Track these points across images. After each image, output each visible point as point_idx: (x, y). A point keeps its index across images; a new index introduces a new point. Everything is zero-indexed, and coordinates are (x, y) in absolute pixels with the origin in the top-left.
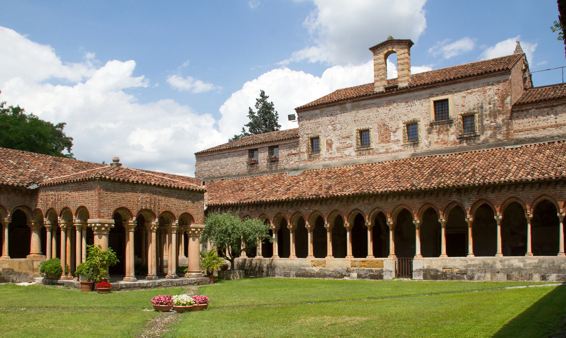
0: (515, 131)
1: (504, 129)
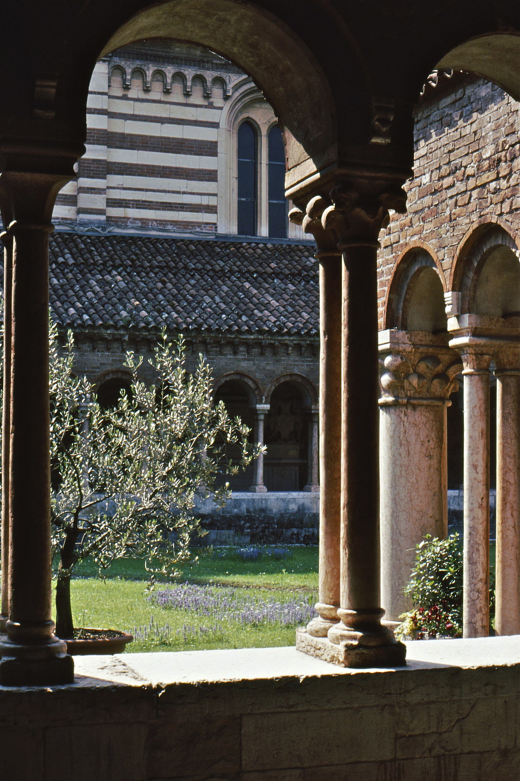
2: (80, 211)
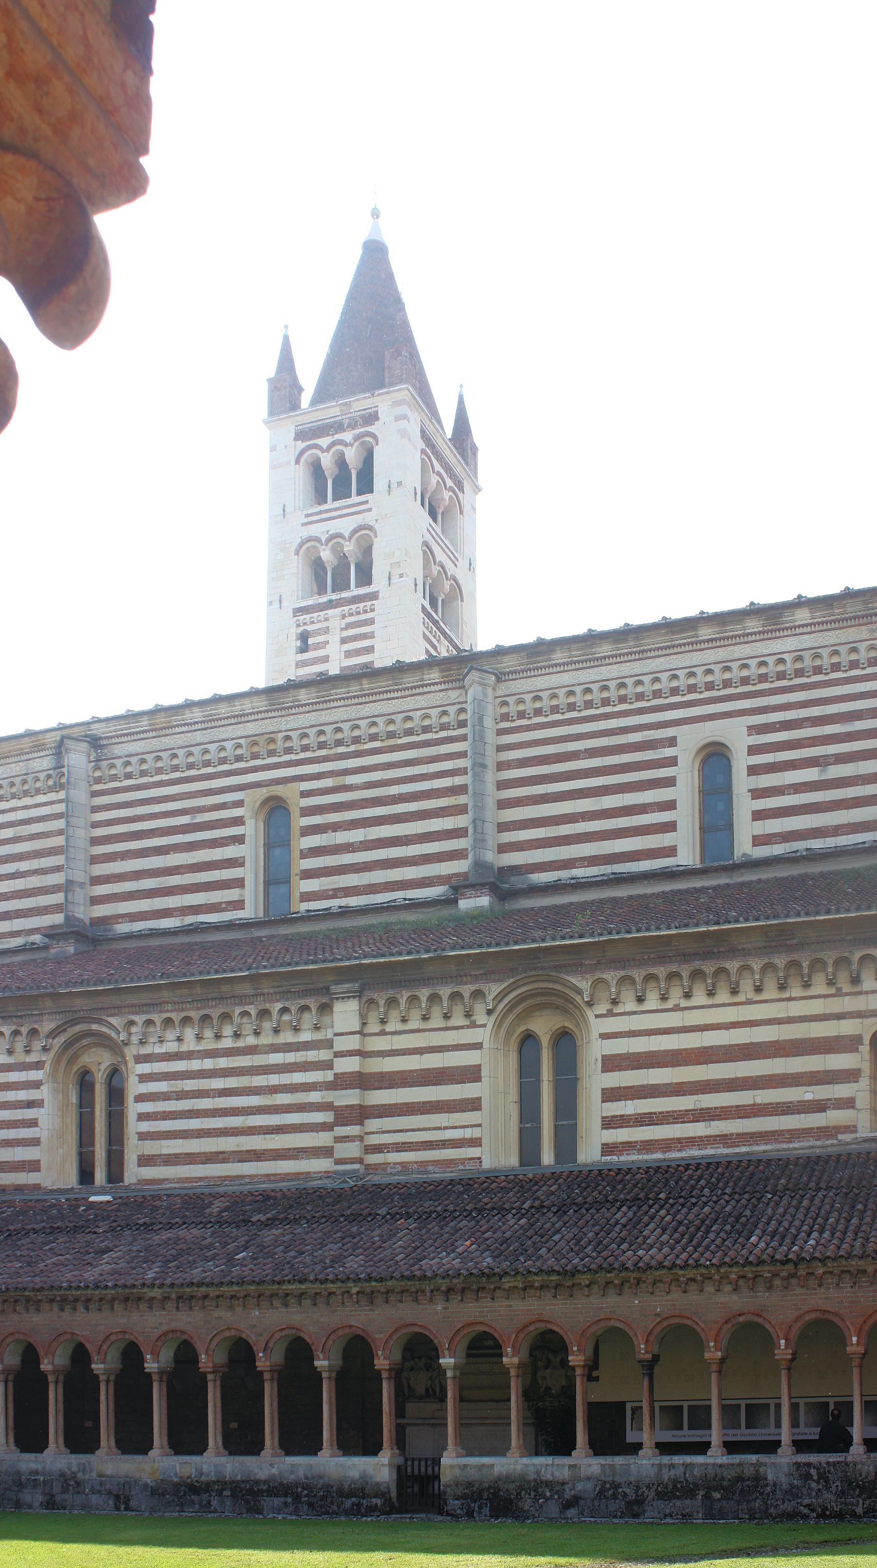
2: (338, 1162)
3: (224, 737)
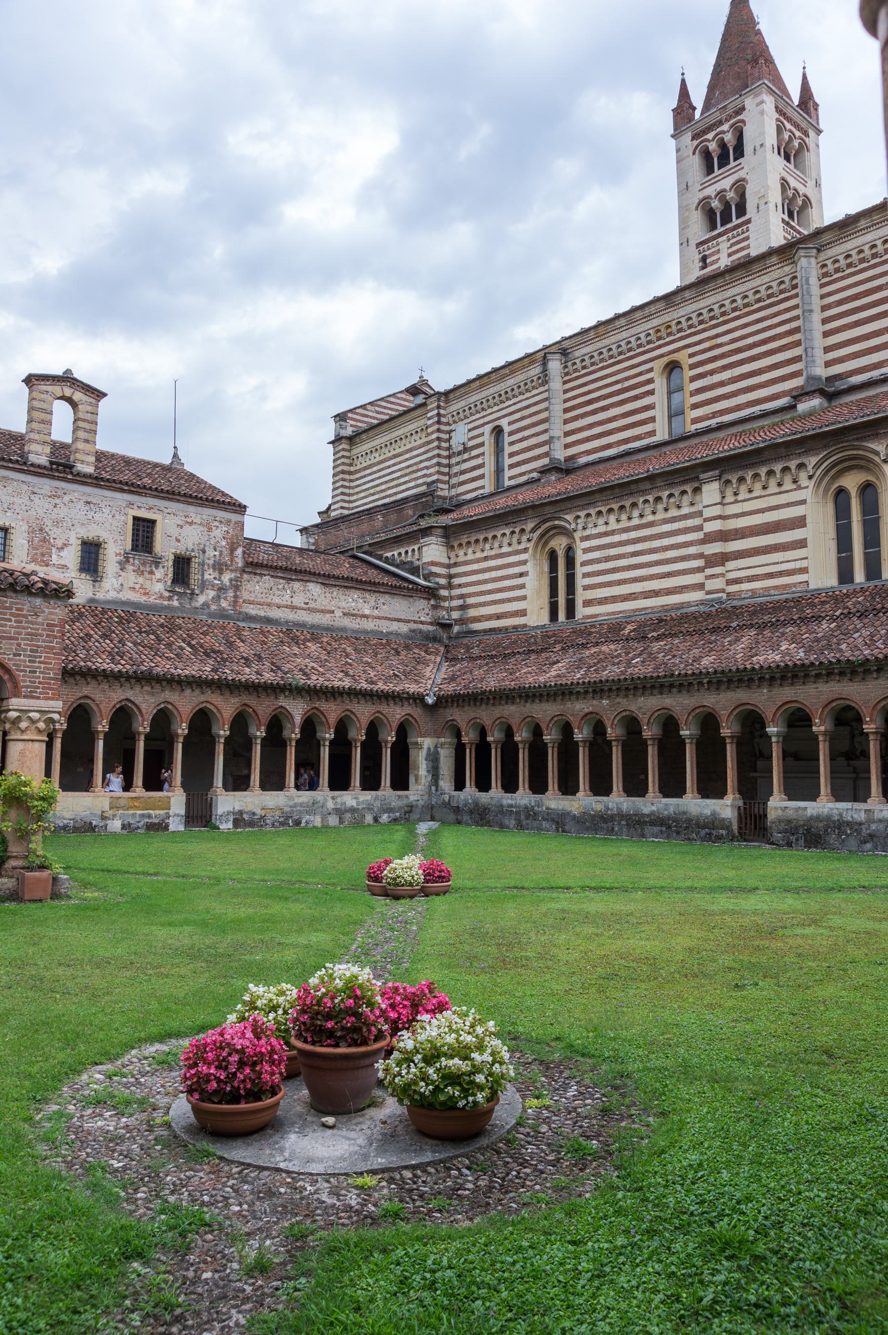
0: (244, 602)
1: (231, 594)
2: (708, 593)
3: (639, 331)
